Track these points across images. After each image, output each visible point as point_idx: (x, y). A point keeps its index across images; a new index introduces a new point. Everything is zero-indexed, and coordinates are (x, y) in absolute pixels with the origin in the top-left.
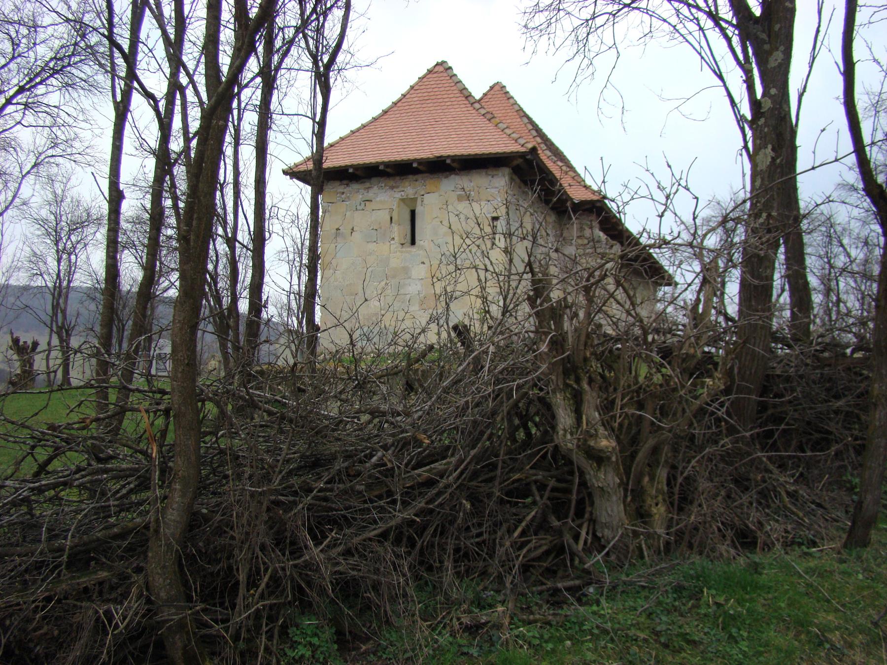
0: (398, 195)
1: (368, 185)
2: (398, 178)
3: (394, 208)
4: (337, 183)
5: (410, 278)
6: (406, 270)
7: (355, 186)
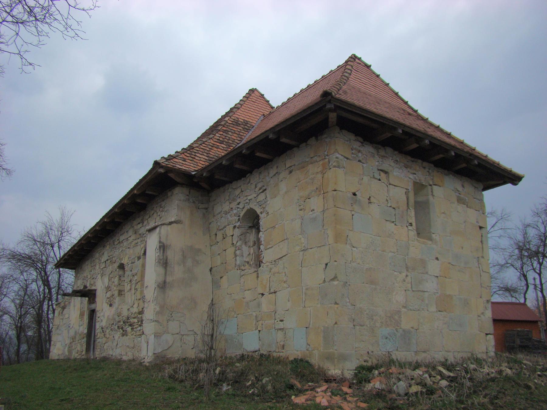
0: (411, 176)
1: (382, 152)
2: (409, 158)
3: (409, 188)
4: (352, 137)
5: (427, 273)
6: (423, 263)
7: (368, 149)
